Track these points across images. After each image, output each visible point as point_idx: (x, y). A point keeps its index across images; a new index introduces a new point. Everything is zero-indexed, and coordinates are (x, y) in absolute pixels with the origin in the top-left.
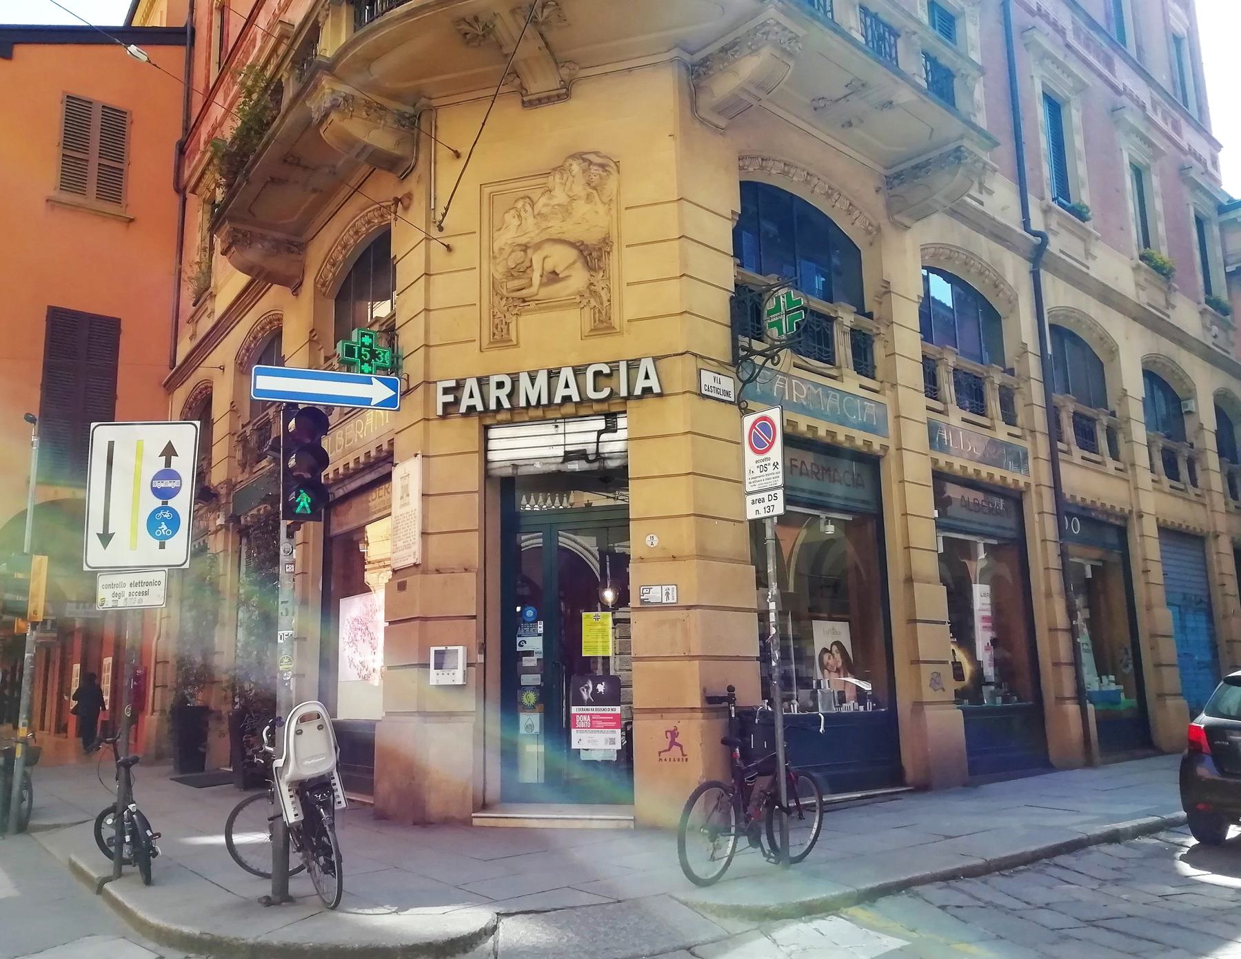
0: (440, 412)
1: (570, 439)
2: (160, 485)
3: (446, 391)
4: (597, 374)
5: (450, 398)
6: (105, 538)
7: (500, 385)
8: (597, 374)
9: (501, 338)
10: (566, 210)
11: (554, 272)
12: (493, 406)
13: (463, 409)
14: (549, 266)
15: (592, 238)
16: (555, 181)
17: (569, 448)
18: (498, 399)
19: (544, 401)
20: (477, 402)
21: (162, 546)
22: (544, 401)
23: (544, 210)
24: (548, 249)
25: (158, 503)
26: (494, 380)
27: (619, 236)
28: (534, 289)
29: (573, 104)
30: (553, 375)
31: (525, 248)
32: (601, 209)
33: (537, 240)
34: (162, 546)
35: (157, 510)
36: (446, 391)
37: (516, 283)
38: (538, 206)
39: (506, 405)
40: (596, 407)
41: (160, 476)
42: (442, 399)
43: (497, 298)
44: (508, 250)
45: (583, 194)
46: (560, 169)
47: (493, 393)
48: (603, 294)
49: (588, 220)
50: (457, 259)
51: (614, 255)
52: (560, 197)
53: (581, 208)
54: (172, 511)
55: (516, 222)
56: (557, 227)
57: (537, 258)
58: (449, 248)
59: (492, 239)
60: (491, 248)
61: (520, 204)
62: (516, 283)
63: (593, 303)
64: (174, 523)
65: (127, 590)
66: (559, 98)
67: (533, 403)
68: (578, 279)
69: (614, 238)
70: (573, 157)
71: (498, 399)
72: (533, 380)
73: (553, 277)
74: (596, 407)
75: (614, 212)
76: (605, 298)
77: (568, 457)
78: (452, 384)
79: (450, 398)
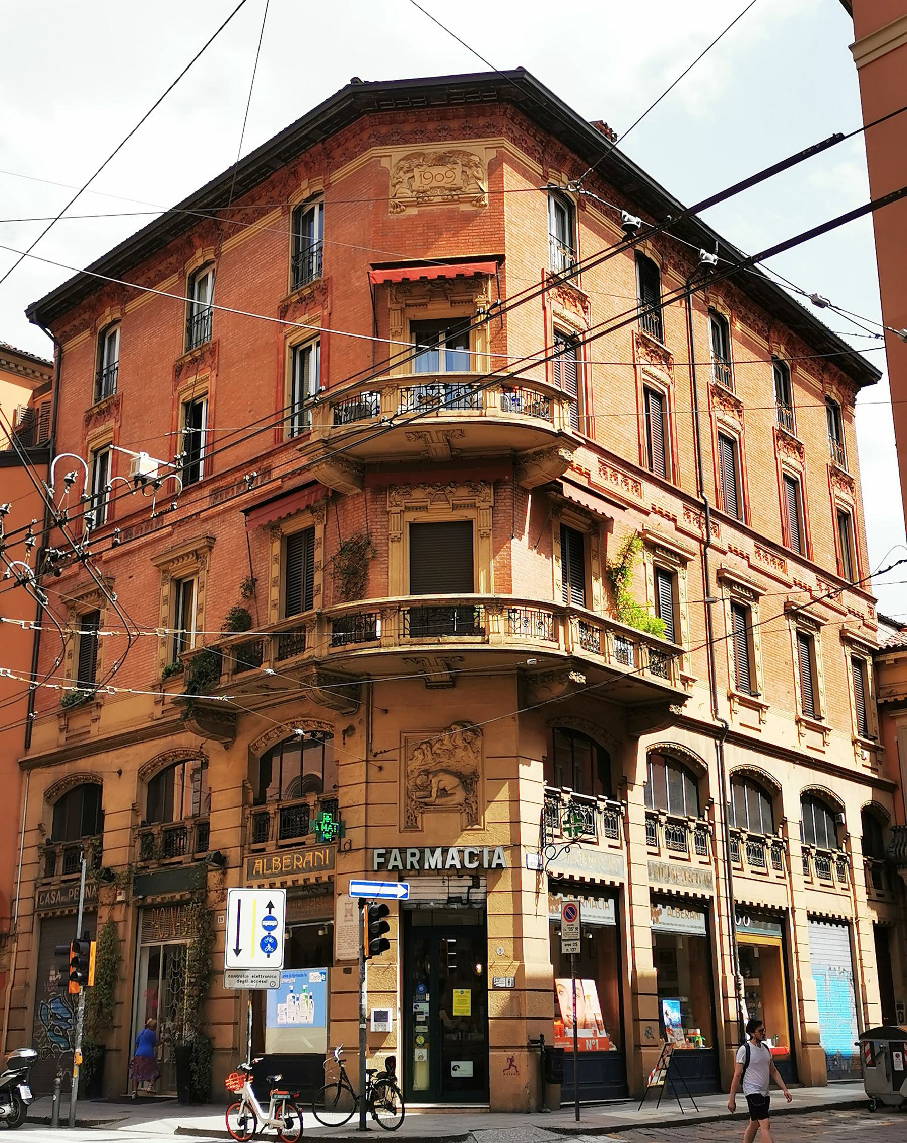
0: (376, 868)
1: (452, 890)
2: (267, 923)
3: (380, 856)
4: (471, 854)
5: (382, 860)
6: (237, 951)
7: (413, 855)
8: (471, 854)
9: (411, 825)
10: (451, 752)
11: (444, 789)
12: (409, 867)
13: (390, 868)
14: (441, 786)
15: (467, 771)
16: (445, 736)
17: (451, 895)
18: (412, 863)
19: (440, 867)
20: (399, 863)
21: (268, 956)
22: (440, 867)
23: (438, 751)
24: (442, 776)
25: (266, 933)
26: (409, 851)
27: (483, 773)
28: (432, 799)
29: (455, 691)
30: (445, 851)
31: (427, 773)
32: (471, 754)
33: (434, 769)
34: (268, 956)
35: (266, 937)
36: (380, 856)
37: (422, 794)
38: (435, 748)
39: (417, 867)
40: (468, 872)
41: (266, 919)
42: (377, 860)
43: (409, 801)
44: (416, 773)
45: (461, 745)
46: (448, 729)
47: (409, 859)
48: (473, 805)
49: (465, 759)
50: (384, 775)
51: (480, 783)
52: (448, 744)
53: (460, 753)
54: (273, 938)
55: (421, 757)
56: (445, 761)
57: (434, 781)
58: (381, 768)
59: (406, 766)
60: (405, 769)
61: (424, 746)
62: (422, 794)
63: (467, 810)
64: (274, 945)
65: (250, 979)
66: (449, 686)
67: (433, 867)
68: (459, 796)
69: (480, 771)
70: (456, 723)
71: (412, 863)
72: (433, 853)
73: (443, 792)
74: (468, 872)
75: (479, 758)
76: (474, 808)
77: (450, 900)
78: (384, 851)
79: (382, 860)
